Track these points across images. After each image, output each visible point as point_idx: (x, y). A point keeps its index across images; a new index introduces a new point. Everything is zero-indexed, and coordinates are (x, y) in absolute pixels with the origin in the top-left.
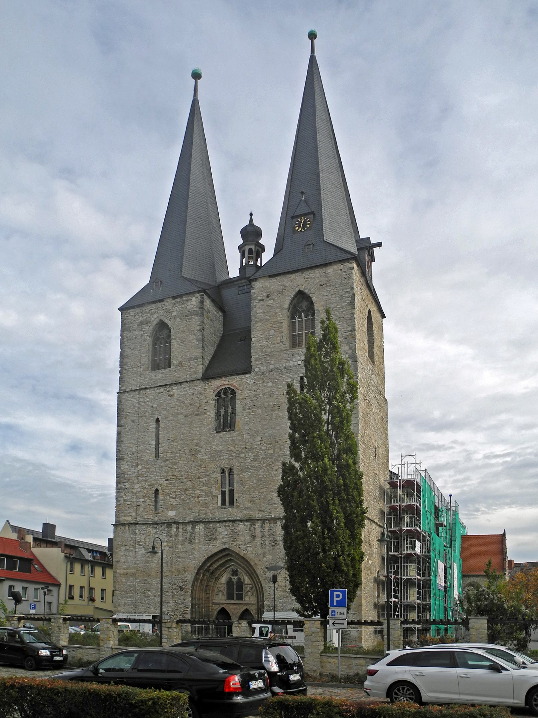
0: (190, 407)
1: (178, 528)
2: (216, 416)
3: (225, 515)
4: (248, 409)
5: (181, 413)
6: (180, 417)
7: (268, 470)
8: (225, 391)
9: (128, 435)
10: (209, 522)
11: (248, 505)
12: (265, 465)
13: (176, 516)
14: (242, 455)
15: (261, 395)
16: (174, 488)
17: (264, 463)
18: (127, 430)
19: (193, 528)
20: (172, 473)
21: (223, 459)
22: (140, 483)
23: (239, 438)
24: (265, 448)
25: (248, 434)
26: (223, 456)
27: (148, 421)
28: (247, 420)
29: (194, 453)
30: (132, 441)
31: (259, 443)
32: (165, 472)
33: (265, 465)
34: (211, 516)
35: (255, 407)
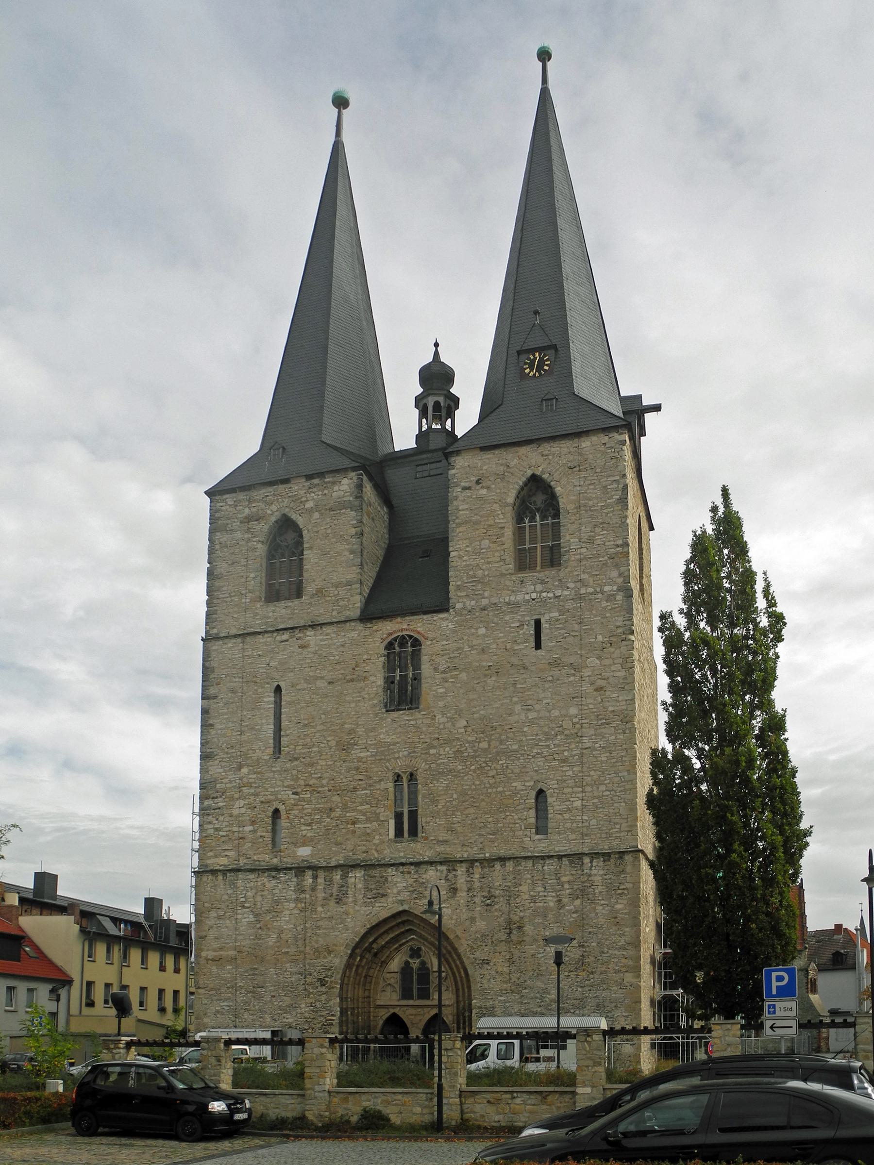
0: (338, 667)
1: (315, 877)
2: (385, 683)
3: (402, 854)
4: (444, 672)
5: (322, 678)
6: (320, 684)
7: (478, 776)
8: (403, 641)
9: (223, 714)
10: (373, 866)
11: (443, 836)
12: (473, 767)
13: (312, 855)
14: (432, 751)
16: (309, 808)
17: (471, 765)
18: (221, 704)
19: (344, 877)
20: (305, 781)
21: (398, 758)
22: (245, 798)
23: (428, 721)
24: (474, 739)
25: (443, 714)
26: (398, 752)
27: (260, 690)
28: (442, 690)
29: (345, 747)
30: (230, 725)
31: (463, 730)
32: (292, 780)
33: (473, 767)
34: (376, 855)
35: (455, 668)
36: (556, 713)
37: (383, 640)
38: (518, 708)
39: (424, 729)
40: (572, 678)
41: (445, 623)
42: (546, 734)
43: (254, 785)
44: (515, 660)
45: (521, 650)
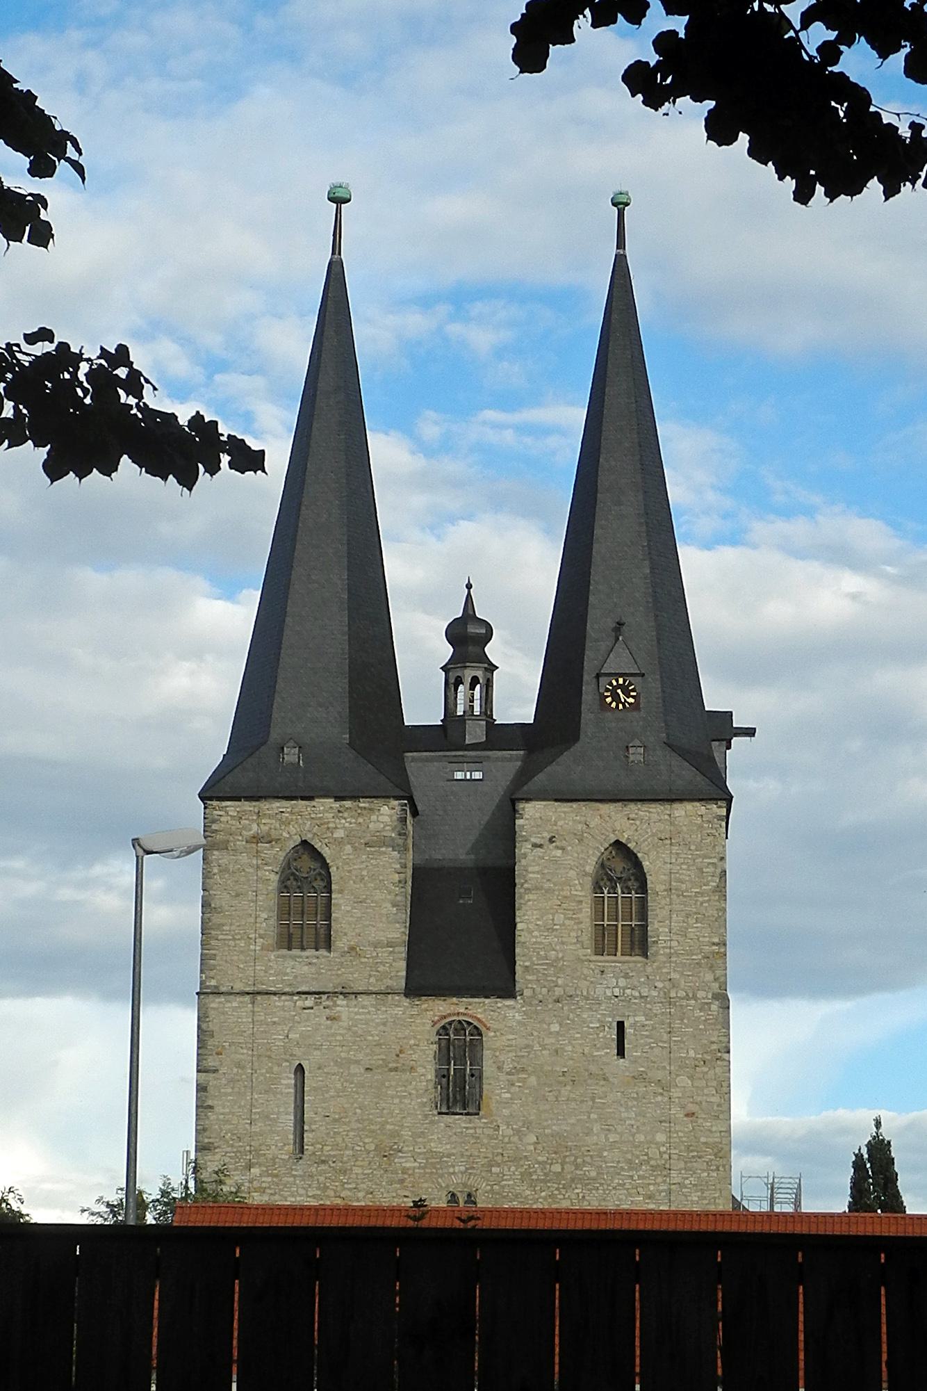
0: (377, 1050)
5: (357, 1062)
6: (355, 1069)
8: (461, 1027)
9: (226, 1094)
15: (537, 1047)
21: (454, 1173)
23: (491, 1132)
25: (508, 1125)
28: (508, 1095)
31: (532, 1148)
35: (523, 1070)
36: (642, 1138)
37: (435, 1023)
38: (596, 1128)
39: (485, 1141)
40: (659, 1098)
41: (510, 1013)
42: (630, 1162)
43: (268, 1191)
44: (593, 1068)
45: (600, 1056)
